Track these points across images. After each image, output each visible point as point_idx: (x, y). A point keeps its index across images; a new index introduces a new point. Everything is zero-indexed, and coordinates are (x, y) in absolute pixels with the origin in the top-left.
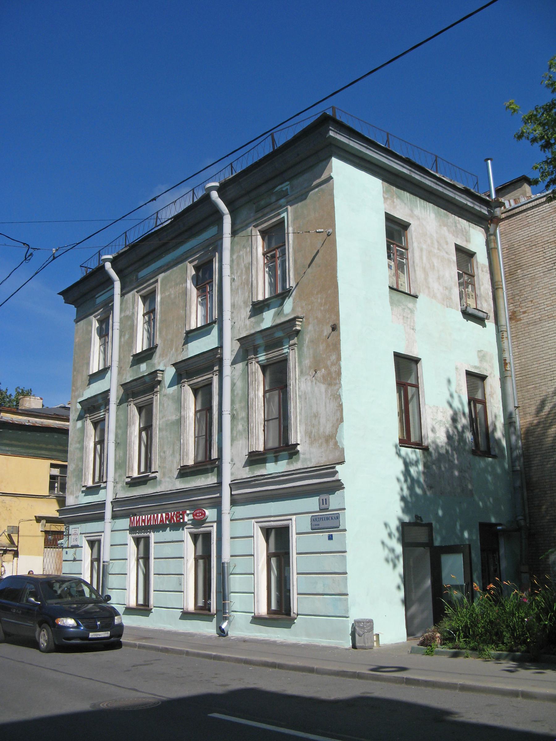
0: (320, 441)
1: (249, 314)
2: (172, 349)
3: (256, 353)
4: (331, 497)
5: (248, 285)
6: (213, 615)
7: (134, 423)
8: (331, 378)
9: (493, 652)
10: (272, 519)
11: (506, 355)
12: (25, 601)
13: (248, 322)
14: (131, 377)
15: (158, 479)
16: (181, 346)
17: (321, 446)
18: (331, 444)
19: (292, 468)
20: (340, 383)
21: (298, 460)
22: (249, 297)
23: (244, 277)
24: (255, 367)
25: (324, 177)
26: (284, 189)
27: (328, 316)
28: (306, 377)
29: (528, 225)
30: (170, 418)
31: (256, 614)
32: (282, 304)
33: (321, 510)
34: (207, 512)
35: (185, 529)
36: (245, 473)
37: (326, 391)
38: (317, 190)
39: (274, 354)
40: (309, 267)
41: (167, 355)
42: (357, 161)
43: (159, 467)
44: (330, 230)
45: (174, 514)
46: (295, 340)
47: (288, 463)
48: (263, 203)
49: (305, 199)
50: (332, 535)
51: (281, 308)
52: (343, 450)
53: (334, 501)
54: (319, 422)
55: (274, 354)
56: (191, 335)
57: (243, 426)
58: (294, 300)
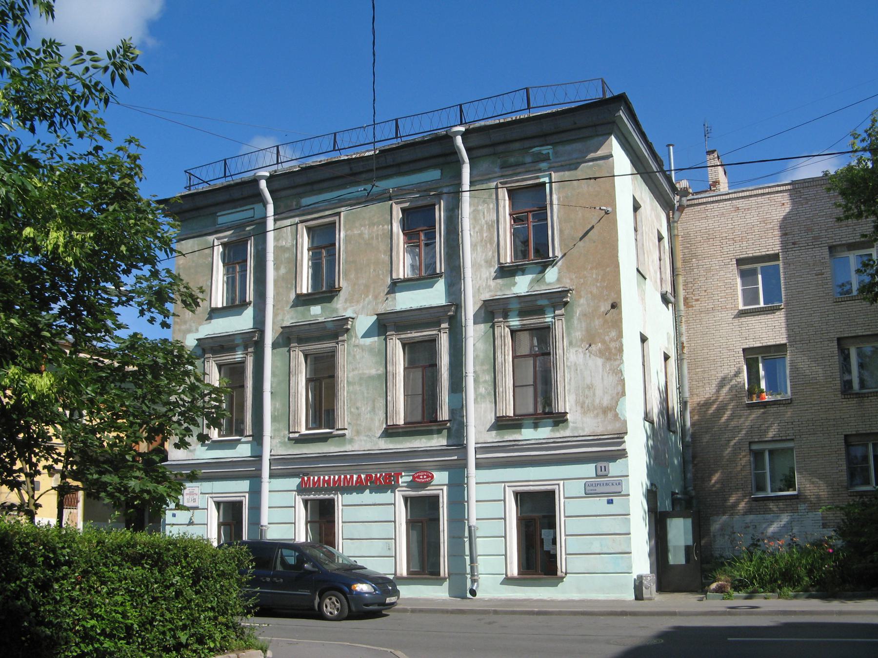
0: (595, 412)
1: (493, 275)
2: (367, 296)
3: (506, 316)
4: (611, 464)
5: (491, 244)
6: (445, 579)
7: (301, 372)
8: (610, 353)
9: (790, 593)
10: (531, 483)
11: (684, 339)
12: (279, 568)
13: (492, 283)
14: (292, 318)
15: (347, 436)
16: (382, 294)
17: (597, 415)
18: (610, 415)
19: (558, 435)
20: (621, 358)
21: (567, 427)
22: (493, 256)
23: (485, 235)
24: (503, 332)
25: (600, 153)
26: (544, 152)
27: (605, 293)
28: (576, 349)
29: (706, 218)
30: (367, 372)
31: (509, 575)
32: (543, 271)
33: (597, 476)
34: (436, 474)
35: (397, 492)
36: (493, 437)
37: (604, 365)
38: (591, 163)
39: (532, 321)
40: (581, 239)
41: (358, 302)
42: (623, 141)
43: (349, 424)
44: (610, 209)
45: (381, 475)
46: (562, 311)
47: (552, 431)
48: (512, 160)
49: (576, 169)
50: (612, 500)
51: (540, 276)
52: (625, 422)
53: (614, 468)
54: (594, 394)
55: (532, 321)
56: (396, 286)
57: (486, 389)
58: (559, 270)
